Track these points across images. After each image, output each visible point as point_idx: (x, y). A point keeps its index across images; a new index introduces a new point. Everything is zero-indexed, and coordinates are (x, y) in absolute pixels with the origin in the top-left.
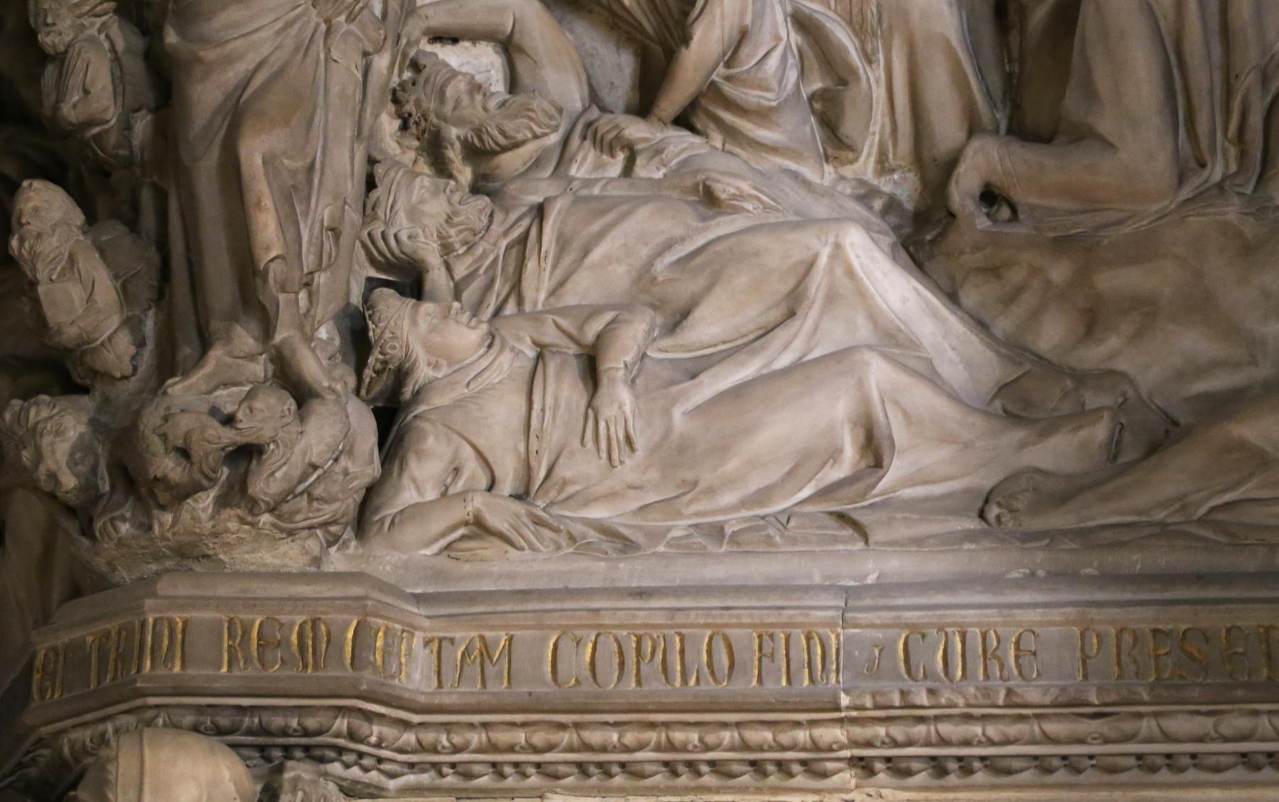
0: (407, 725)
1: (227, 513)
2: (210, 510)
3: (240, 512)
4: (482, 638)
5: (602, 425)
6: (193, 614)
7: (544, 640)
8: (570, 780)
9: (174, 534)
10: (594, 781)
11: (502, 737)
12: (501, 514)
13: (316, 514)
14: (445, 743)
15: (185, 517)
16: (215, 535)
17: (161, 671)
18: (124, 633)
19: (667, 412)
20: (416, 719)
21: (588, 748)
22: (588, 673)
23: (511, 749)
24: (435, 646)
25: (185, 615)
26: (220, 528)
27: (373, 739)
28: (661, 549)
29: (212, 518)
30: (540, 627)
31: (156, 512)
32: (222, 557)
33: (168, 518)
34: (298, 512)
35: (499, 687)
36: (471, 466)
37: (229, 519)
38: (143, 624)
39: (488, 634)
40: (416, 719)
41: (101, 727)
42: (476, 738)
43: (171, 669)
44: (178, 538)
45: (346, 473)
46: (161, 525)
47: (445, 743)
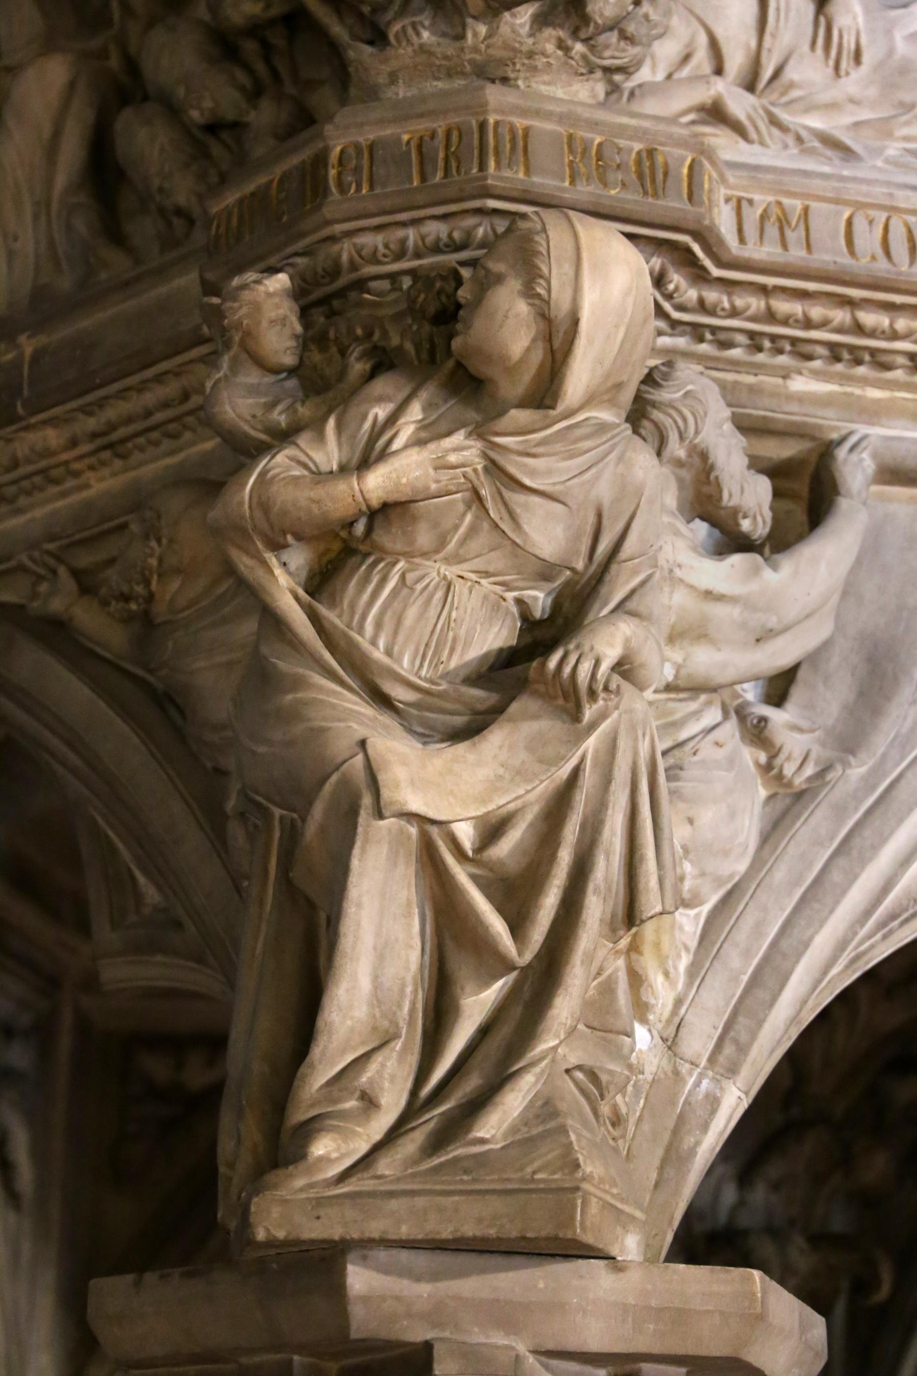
0: (700, 276)
1: (549, 32)
2: (527, 28)
3: (561, 33)
4: (779, 203)
5: (835, 33)
6: (536, 123)
7: (839, 214)
8: (817, 364)
9: (488, 47)
10: (839, 367)
11: (783, 306)
12: (740, 105)
13: (623, 55)
14: (726, 305)
15: (504, 29)
16: (531, 55)
17: (507, 173)
18: (455, 134)
19: (889, 33)
20: (716, 272)
21: (859, 329)
22: (879, 252)
23: (785, 322)
24: (734, 203)
25: (526, 122)
26: (539, 47)
27: (671, 287)
28: (879, 163)
29: (531, 35)
30: (837, 201)
31: (469, 21)
32: (520, 83)
33: (482, 29)
34: (607, 47)
35: (797, 254)
36: (702, 55)
37: (548, 40)
38: (483, 126)
39: (786, 201)
40: (716, 272)
41: (400, 233)
42: (756, 304)
43: (517, 172)
44: (491, 51)
45: (646, 17)
46: (475, 35)
47: (726, 305)
